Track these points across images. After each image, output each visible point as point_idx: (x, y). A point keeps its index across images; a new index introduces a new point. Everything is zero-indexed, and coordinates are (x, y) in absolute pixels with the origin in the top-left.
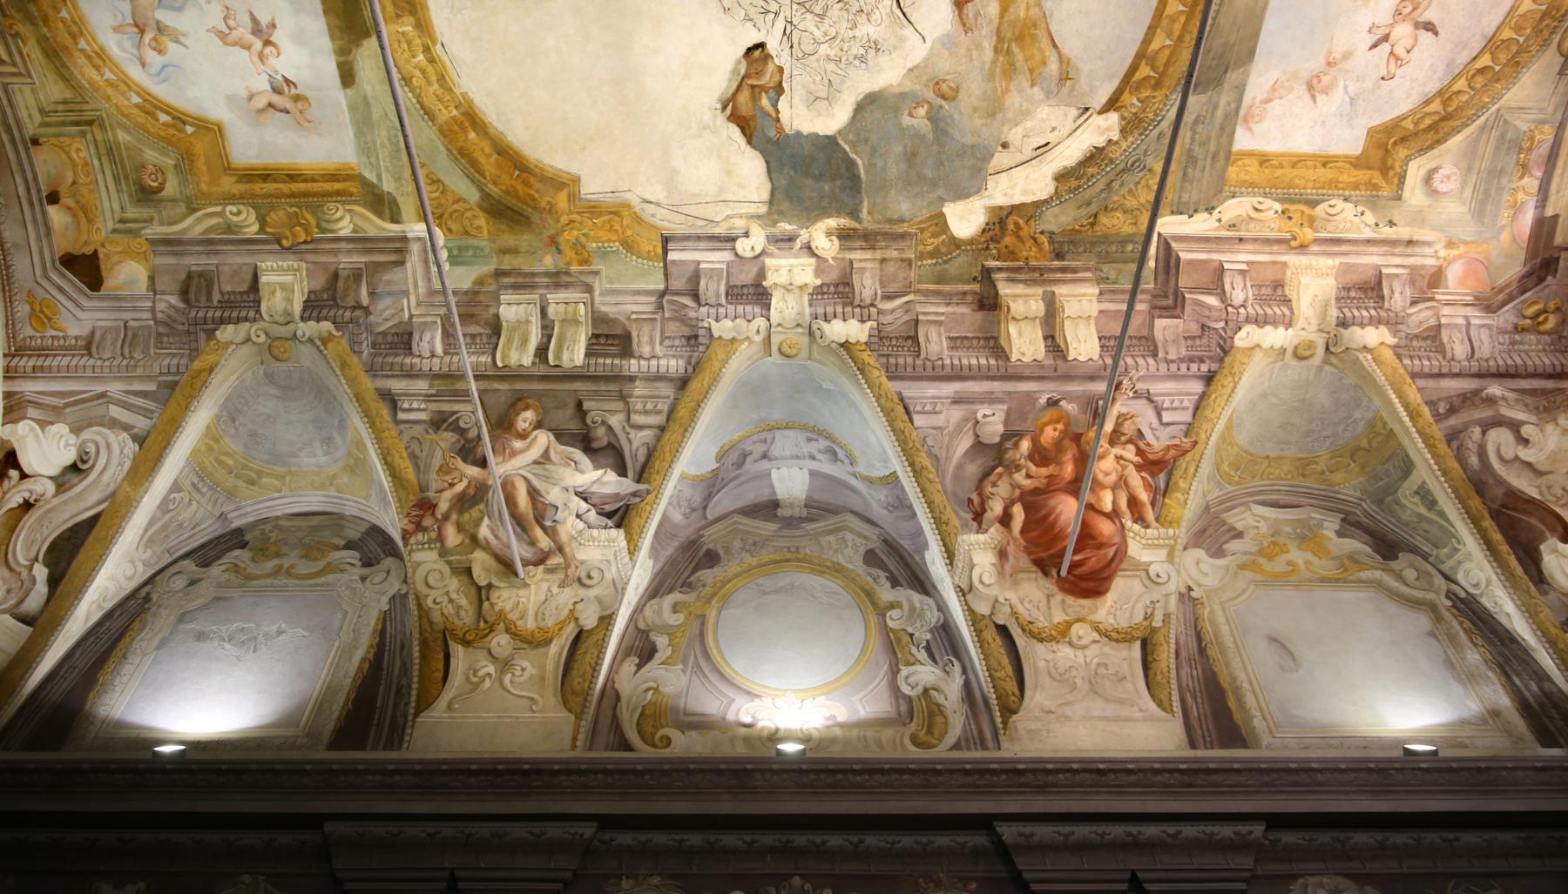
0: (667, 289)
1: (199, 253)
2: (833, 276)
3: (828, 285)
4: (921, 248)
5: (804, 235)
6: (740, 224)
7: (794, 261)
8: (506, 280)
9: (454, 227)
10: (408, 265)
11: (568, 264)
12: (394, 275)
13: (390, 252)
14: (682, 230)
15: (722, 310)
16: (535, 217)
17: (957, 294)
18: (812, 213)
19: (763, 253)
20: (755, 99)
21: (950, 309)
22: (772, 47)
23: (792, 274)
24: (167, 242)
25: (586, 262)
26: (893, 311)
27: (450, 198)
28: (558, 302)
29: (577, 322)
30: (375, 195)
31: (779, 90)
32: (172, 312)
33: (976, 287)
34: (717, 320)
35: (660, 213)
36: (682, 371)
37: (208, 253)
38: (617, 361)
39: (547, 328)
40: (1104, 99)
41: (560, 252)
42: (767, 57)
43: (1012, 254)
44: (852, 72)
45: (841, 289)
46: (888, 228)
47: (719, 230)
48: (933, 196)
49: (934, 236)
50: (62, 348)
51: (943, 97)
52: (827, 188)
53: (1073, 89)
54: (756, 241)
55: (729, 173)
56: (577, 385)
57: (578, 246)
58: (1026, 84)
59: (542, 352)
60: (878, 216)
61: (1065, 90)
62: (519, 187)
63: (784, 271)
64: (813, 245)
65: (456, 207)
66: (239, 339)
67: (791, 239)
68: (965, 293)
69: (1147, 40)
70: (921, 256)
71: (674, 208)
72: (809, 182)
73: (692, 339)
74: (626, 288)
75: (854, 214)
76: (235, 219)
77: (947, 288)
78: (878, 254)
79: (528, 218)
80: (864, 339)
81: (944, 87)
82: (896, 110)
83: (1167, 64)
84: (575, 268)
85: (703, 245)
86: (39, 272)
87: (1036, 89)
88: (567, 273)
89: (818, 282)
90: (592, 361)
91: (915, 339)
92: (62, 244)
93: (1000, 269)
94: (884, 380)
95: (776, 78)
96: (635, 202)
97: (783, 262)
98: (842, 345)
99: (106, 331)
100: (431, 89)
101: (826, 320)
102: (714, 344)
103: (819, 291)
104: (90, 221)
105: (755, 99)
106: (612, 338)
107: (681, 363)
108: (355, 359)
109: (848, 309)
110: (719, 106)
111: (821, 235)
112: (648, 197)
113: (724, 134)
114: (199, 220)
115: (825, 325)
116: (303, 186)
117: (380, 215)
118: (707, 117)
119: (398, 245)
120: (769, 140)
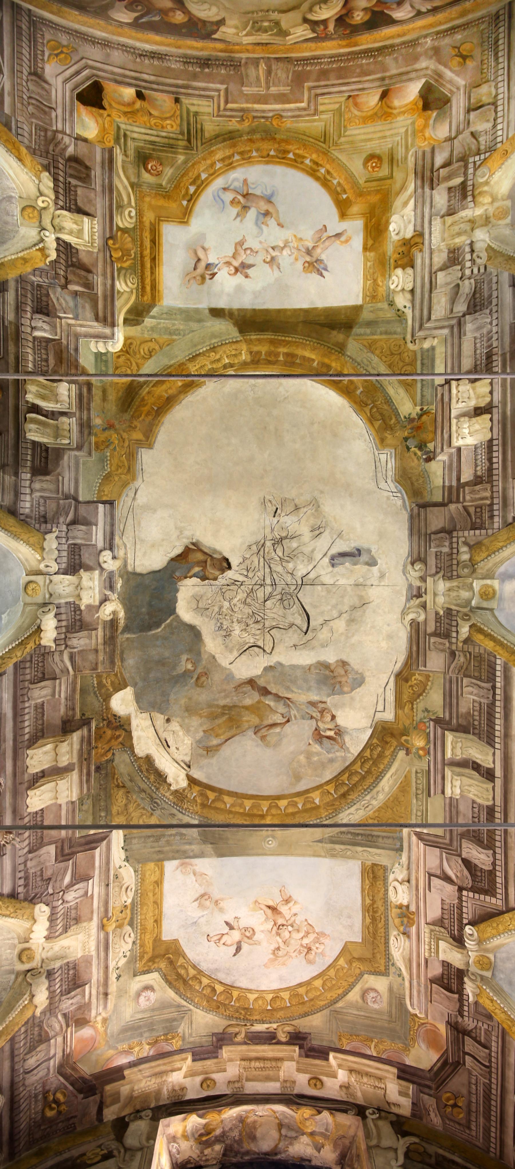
0: (79, 502)
1: (103, 180)
2: (87, 618)
3: (80, 615)
4: (105, 675)
5: (114, 596)
6: (121, 553)
7: (97, 590)
10: (96, 324)
11: (96, 435)
12: (89, 313)
14: (117, 514)
15: (64, 541)
16: (127, 416)
17: (74, 704)
18: (127, 601)
19: (102, 569)
21: (63, 700)
22: (229, 574)
23: (90, 588)
24: (111, 161)
25: (97, 447)
26: (62, 661)
27: (139, 361)
28: (70, 424)
29: (57, 436)
30: (142, 312)
31: (204, 578)
32: (62, 146)
33: (78, 716)
34: (57, 537)
35: (129, 500)
36: (22, 511)
37: (103, 186)
38: (29, 464)
39: (53, 415)
40: (195, 776)
42: (223, 571)
44: (213, 622)
45: (78, 624)
46: (118, 652)
47: (117, 540)
48: (138, 679)
49: (112, 683)
51: (198, 678)
52: (144, 610)
53: (201, 756)
54: (110, 564)
55: (153, 546)
56: (12, 432)
57: (108, 443)
58: (205, 727)
59: (35, 409)
60: (125, 645)
61: (201, 751)
62: (146, 409)
63: (90, 584)
64: (107, 603)
65: (134, 364)
66: (42, 188)
67: (111, 588)
68: (74, 709)
69: (230, 794)
70: (99, 676)
71: (131, 509)
72: (147, 599)
73: (44, 519)
74: (79, 474)
75: (127, 629)
76: (127, 213)
77: (77, 696)
78: (100, 647)
79: (126, 411)
80: (44, 642)
82: (190, 651)
83: (216, 809)
84: (93, 439)
85: (108, 528)
86: (90, 63)
87: (202, 734)
88: (90, 434)
89: (83, 608)
90: (29, 446)
91: (43, 679)
92: (109, 87)
93: (89, 731)
94: (15, 660)
95: (211, 576)
96: (138, 483)
97: (97, 583)
98: (39, 627)
99: (48, 93)
101: (56, 615)
102: (40, 535)
103: (76, 608)
104: (125, 113)
106: (45, 461)
107: (27, 511)
108: (29, 269)
109: (64, 630)
111: (113, 608)
113: (177, 544)
114: (125, 188)
115: (52, 615)
116: (148, 265)
118: (187, 533)
119: (109, 319)
120: (173, 572)
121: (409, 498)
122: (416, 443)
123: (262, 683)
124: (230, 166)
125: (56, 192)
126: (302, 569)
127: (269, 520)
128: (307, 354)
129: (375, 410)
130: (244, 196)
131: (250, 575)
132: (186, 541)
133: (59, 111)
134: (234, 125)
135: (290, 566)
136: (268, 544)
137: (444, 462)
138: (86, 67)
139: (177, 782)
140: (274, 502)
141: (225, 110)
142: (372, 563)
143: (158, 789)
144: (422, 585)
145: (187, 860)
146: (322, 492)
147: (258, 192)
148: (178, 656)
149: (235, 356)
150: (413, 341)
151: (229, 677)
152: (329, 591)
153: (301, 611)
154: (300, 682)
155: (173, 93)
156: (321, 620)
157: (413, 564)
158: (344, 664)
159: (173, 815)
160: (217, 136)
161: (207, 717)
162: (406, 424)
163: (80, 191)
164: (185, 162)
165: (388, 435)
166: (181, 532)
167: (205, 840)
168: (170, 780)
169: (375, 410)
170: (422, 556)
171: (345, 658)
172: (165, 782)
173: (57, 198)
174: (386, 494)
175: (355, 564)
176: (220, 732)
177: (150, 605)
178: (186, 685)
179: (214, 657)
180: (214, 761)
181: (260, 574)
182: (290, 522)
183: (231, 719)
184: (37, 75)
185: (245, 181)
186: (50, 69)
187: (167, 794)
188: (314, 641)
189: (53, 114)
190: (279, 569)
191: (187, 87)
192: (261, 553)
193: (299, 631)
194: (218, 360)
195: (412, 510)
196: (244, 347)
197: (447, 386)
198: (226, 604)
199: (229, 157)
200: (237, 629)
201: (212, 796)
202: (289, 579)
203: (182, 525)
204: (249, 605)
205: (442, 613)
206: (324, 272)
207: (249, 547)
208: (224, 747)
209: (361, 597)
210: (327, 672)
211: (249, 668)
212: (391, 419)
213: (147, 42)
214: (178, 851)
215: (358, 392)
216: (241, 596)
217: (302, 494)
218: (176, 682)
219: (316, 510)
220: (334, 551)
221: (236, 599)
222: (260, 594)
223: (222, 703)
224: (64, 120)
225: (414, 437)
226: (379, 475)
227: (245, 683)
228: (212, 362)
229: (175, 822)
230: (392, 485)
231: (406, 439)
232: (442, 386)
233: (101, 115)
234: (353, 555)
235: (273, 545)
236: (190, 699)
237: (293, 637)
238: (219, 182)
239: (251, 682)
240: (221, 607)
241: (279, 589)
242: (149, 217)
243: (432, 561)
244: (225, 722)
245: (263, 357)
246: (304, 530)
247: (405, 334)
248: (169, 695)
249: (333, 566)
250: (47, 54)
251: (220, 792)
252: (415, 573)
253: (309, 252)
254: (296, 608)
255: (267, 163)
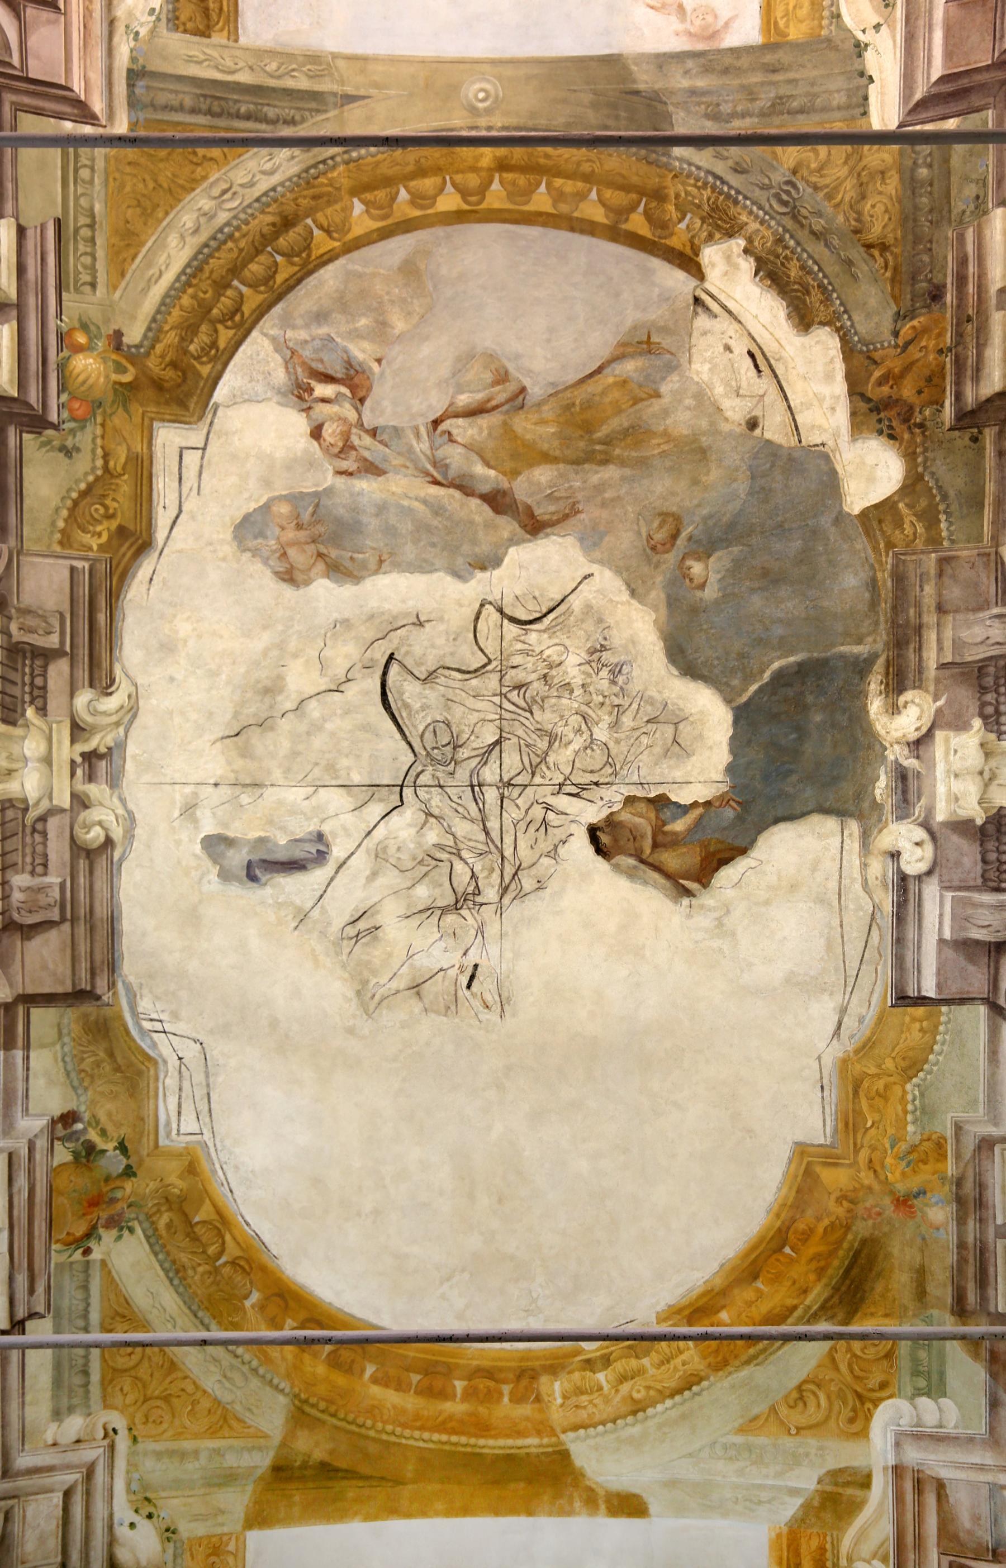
0: (986, 1001)
2: (966, 697)
3: (983, 705)
4: (919, 545)
5: (896, 753)
6: (877, 867)
8: (972, 1297)
9: (875, 1379)
13: (920, 1504)
14: (886, 972)
16: (862, 1228)
18: (859, 741)
19: (926, 825)
20: (674, 842)
22: (593, 814)
27: (830, 1374)
30: (823, 1507)
31: (661, 802)
33: (989, 435)
35: (856, 1008)
40: (680, 275)
41: (922, 1193)
42: (611, 822)
43: (933, 380)
44: (635, 687)
45: (989, 681)
46: (885, 607)
47: (887, 902)
49: (899, 524)
51: (674, 536)
52: (818, 718)
53: (665, 330)
54: (904, 837)
55: (794, 887)
58: (656, 405)
60: (866, 626)
62: (812, 1249)
63: (957, 786)
64: (913, 736)
65: (843, 1368)
67: (902, 776)
69: (588, 228)
70: (934, 541)
71: (851, 984)
72: (808, 748)
75: (862, 668)
78: (930, 618)
79: (864, 1242)
81: (659, 536)
82: (695, 610)
83: (626, 188)
85: (911, 934)
87: (664, 389)
88: (959, 1182)
89: (977, 723)
93: (959, 396)
95: (642, 807)
96: (833, 1053)
97: (941, 789)
100: (652, 1371)
105: (674, 842)
110: (686, 901)
111: (897, 722)
112: (831, 1028)
113: (730, 893)
117: (855, 1507)
118: (704, 921)
120: (740, 818)
121: (120, 1017)
122: (103, 1162)
123: (507, 526)
126: (403, 825)
127: (489, 957)
128: (391, 1397)
129: (212, 1250)
131: (538, 812)
132: (707, 899)
135: (433, 836)
136: (491, 894)
137: (26, 1111)
139: (728, 258)
140: (477, 1004)
142: (216, 845)
143: (779, 241)
144: (81, 787)
145: (700, 46)
146: (351, 1031)
148: (727, 596)
149: (580, 1391)
150: (110, 1433)
151: (591, 541)
152: (331, 768)
153: (403, 716)
154: (406, 527)
156: (352, 691)
157: (109, 842)
158: (289, 577)
159: (738, 170)
161: (650, 433)
162: (130, 1214)
165: (178, 1184)
166: (720, 923)
167: (654, 103)
168: (747, 265)
169: (212, 1250)
170: (82, 864)
171: (288, 591)
172: (759, 260)
174: (180, 1027)
175: (262, 841)
176: (616, 394)
177: (801, 731)
178: (705, 519)
179: (633, 593)
180: (632, 316)
181: (513, 813)
182: (435, 951)
183: (587, 428)
187: (754, 226)
188: (370, 635)
190: (462, 828)
192: (509, 871)
193: (409, 662)
194: (623, 1378)
195: (112, 985)
196: (557, 1416)
197: (21, 1313)
198: (601, 733)
200: (573, 667)
201: (637, 223)
202: (437, 801)
203: (716, 943)
204: (540, 731)
205: (30, 712)
207: (540, 886)
208: (606, 353)
209: (245, 753)
210: (334, 553)
211: (541, 566)
212: (169, 1226)
214: (726, 71)
215: (255, 1297)
216: (562, 756)
217: (404, 1025)
218: (732, 525)
219: (365, 983)
220: (318, 876)
221: (575, 746)
222: (512, 761)
223: (611, 472)
225: (107, 1179)
226: (199, 1078)
227: (551, 524)
228: (640, 1372)
229: (734, 151)
230: (166, 1051)
231: (129, 1172)
232: (32, 1315)
234: (265, 866)
235: (477, 891)
236: (695, 482)
237: (425, 648)
239: (534, 527)
240: (615, 725)
241: (463, 775)
243: (57, 850)
244: (603, 421)
245: (506, 1389)
246: (396, 931)
247: (132, 1454)
248: (751, 493)
249: (320, 837)
251: (615, 234)
252: (103, 818)
254: (416, 726)
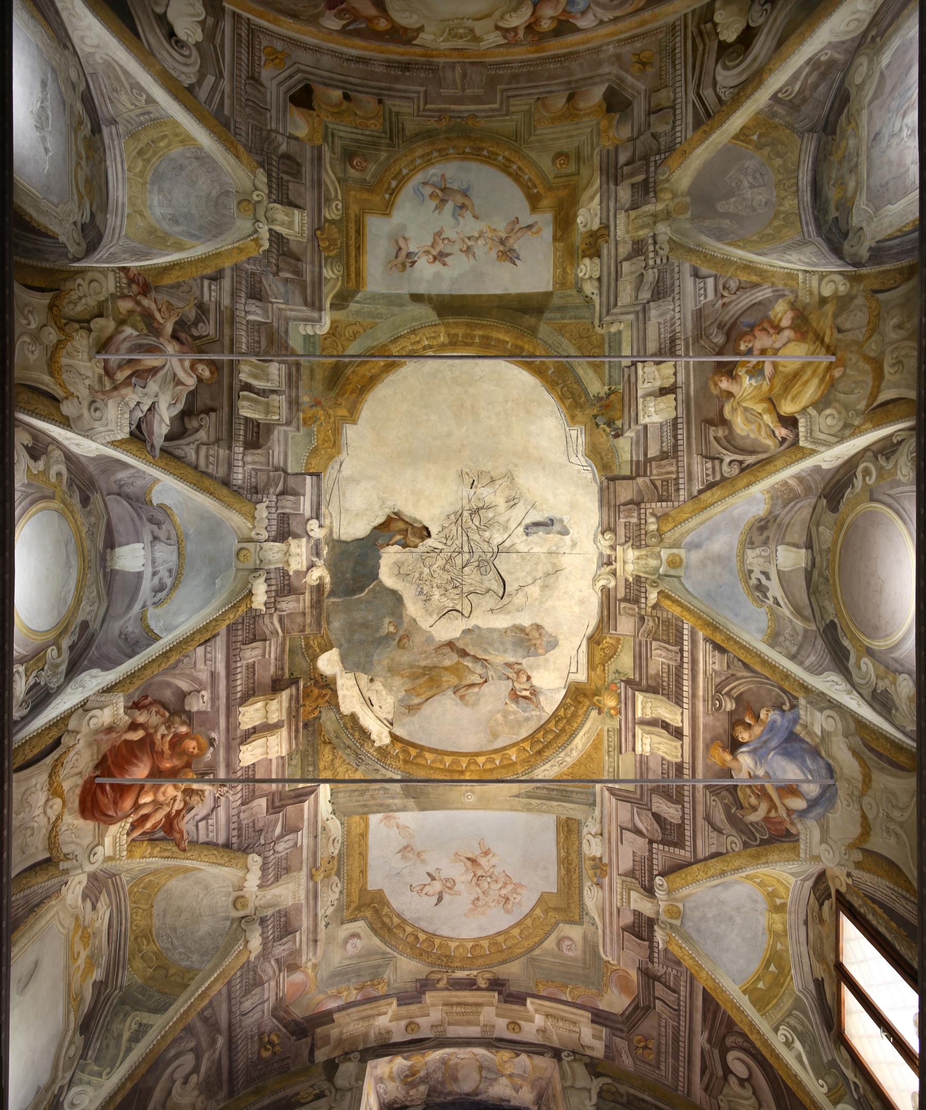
24: (320, 158)
37: (312, 181)
50: (253, 62)
92: (319, 89)
104: (333, 114)
114: (333, 182)
124: (429, 163)
125: (270, 187)
130: (442, 190)
133: (274, 112)
134: (432, 124)
138: (299, 71)
141: (424, 110)
147: (455, 186)
155: (376, 94)
160: (417, 135)
163: (291, 186)
164: (388, 158)
173: (270, 192)
184: (254, 79)
185: (443, 176)
186: (266, 74)
189: (268, 115)
191: (390, 89)
199: (428, 154)
206: (517, 261)
213: (353, 47)
224: (278, 120)
233: (311, 116)
238: (419, 177)
242: (354, 209)
250: (263, 59)
253: (502, 242)
255: (463, 159)
